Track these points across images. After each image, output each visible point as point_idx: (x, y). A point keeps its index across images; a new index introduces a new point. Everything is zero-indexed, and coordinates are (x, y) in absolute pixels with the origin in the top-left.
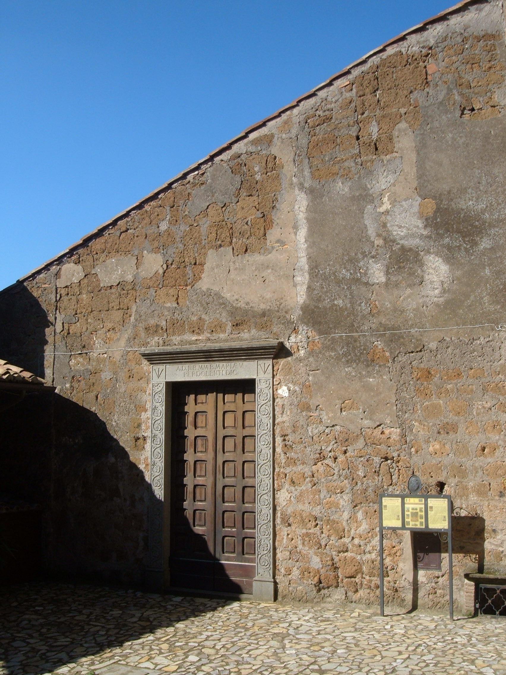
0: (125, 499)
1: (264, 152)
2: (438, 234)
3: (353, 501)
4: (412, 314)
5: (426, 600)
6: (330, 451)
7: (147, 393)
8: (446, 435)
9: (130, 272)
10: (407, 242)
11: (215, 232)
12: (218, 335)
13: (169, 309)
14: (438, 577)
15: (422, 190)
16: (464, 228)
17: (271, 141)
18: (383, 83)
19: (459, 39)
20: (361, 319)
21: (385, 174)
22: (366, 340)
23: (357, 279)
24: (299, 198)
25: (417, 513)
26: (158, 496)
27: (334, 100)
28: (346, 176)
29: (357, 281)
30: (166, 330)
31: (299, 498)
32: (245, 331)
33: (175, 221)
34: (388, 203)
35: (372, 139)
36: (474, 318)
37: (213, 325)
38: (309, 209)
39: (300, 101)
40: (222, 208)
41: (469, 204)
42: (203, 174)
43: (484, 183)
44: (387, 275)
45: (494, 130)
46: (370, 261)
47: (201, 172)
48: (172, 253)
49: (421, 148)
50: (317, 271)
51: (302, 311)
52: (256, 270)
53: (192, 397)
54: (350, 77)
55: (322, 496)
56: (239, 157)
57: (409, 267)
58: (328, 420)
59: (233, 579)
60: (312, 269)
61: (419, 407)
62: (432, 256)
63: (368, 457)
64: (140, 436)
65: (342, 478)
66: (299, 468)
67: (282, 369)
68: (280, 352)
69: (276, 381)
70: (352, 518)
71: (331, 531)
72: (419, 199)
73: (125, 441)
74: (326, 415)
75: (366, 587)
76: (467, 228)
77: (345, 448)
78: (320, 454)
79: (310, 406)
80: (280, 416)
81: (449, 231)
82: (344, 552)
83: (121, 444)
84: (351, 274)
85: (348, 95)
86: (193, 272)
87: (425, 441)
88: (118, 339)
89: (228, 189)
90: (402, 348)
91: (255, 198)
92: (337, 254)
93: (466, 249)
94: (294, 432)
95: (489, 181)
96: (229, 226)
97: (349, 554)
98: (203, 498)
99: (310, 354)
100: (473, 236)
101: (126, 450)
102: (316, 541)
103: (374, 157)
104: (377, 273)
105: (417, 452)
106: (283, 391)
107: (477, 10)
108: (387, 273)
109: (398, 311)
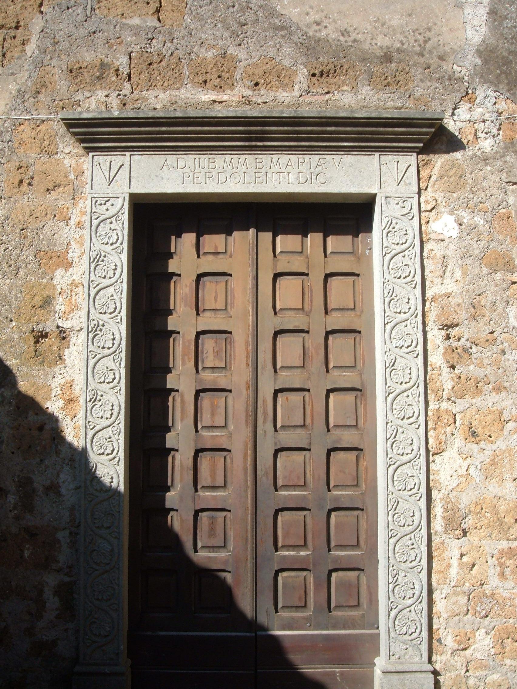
7: (73, 222)
12: (272, 93)
13: (137, 31)
26: (106, 480)
30: (129, 75)
31: (492, 468)
32: (345, 88)
37: (260, 71)
51: (480, 57)
53: (189, 238)
59: (307, 670)
64: (50, 327)
66: (490, 400)
67: (441, 177)
68: (435, 139)
69: (427, 202)
80: (438, 281)
98: (220, 481)
99: (506, 148)
101: (8, 363)
106: (444, 225)
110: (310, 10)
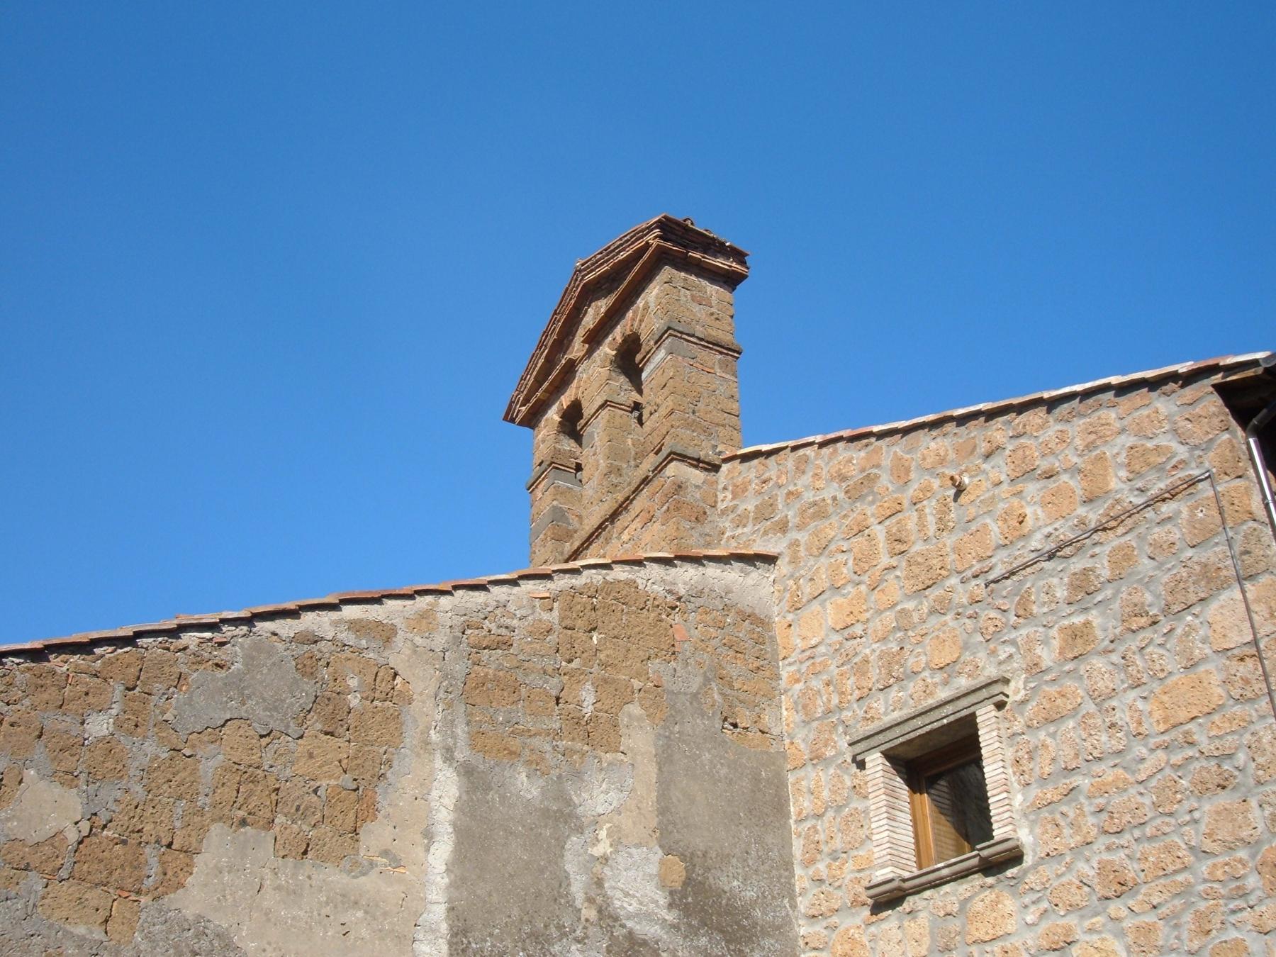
1: (371, 655)
2: (690, 925)
10: (638, 927)
11: (236, 786)
15: (668, 835)
17: (388, 640)
24: (440, 776)
27: (518, 614)
28: (536, 766)
33: (132, 724)
34: (608, 842)
38: (459, 808)
39: (456, 588)
40: (262, 736)
42: (222, 644)
46: (573, 948)
47: (218, 637)
48: (111, 799)
49: (665, 759)
52: (327, 903)
54: (549, 584)
56: (316, 642)
60: (457, 934)
72: (660, 852)
85: (546, 616)
86: (162, 863)
91: (341, 742)
96: (271, 781)
103: (586, 748)
107: (741, 571)
110: (267, 947)
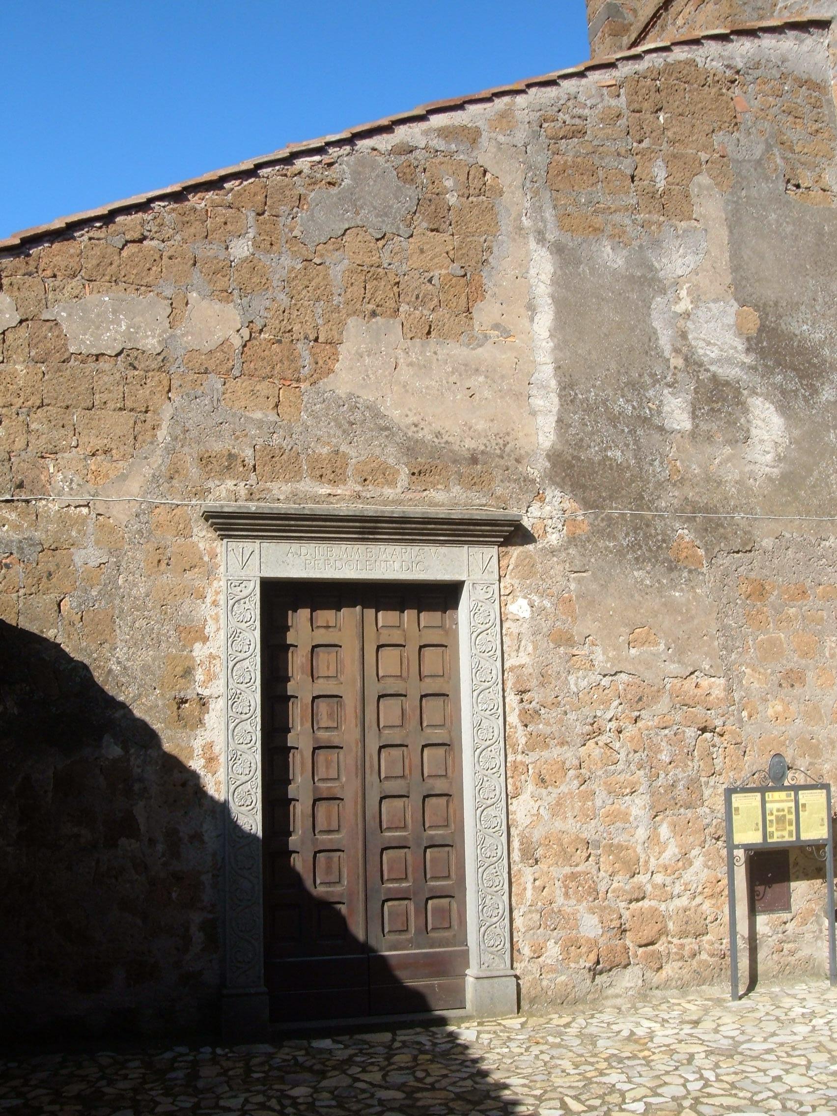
0: (150, 840)
1: (461, 157)
2: (766, 366)
3: (651, 808)
4: (733, 489)
5: (770, 963)
6: (610, 720)
7: (208, 600)
8: (790, 689)
9: (152, 330)
10: (720, 370)
11: (363, 285)
12: (379, 489)
13: (260, 424)
14: (785, 923)
15: (741, 289)
16: (799, 364)
17: (474, 141)
18: (671, 102)
19: (776, 73)
20: (656, 489)
21: (681, 251)
22: (665, 524)
23: (645, 418)
24: (535, 256)
25: (784, 816)
26: (246, 828)
27: (589, 103)
28: (619, 238)
29: (645, 421)
30: (254, 466)
31: (558, 808)
32: (439, 487)
33: (267, 243)
34: (688, 300)
35: (657, 187)
36: (820, 506)
37: (368, 468)
38: (555, 282)
39: (529, 86)
40: (377, 240)
41: (803, 327)
42: (330, 165)
43: (820, 300)
44: (693, 419)
45: (829, 226)
46: (666, 391)
47: (326, 159)
48: (262, 308)
49: (734, 222)
50: (572, 393)
51: (549, 461)
52: (453, 373)
53: (304, 613)
54: (614, 73)
55: (598, 802)
56: (411, 151)
57: (727, 412)
58: (606, 662)
59: (410, 983)
60: (565, 388)
61: (751, 643)
62: (760, 399)
63: (675, 727)
64: (190, 694)
65: (633, 767)
66: (555, 753)
67: (517, 566)
68: (514, 534)
69: (505, 587)
70: (653, 839)
71: (616, 865)
72: (736, 305)
73: (148, 706)
74: (603, 654)
75: (677, 957)
76: (803, 364)
77: (637, 713)
78: (592, 725)
79: (572, 636)
80: (514, 654)
81: (781, 365)
82: (637, 900)
83: (138, 713)
84: (634, 407)
85: (613, 102)
86: (313, 355)
87: (762, 698)
88: (123, 477)
89: (391, 207)
90: (722, 544)
91: (446, 236)
92: (608, 370)
93: (804, 396)
94: (542, 684)
95: (826, 300)
96: (392, 278)
97: (645, 904)
98: (335, 826)
99: (569, 542)
100: (812, 379)
101: (154, 727)
102: (590, 887)
103: (662, 219)
104: (677, 412)
105: (750, 717)
106: (520, 608)
107: (796, 38)
108: (694, 416)
109: (713, 481)
110: (409, 413)
